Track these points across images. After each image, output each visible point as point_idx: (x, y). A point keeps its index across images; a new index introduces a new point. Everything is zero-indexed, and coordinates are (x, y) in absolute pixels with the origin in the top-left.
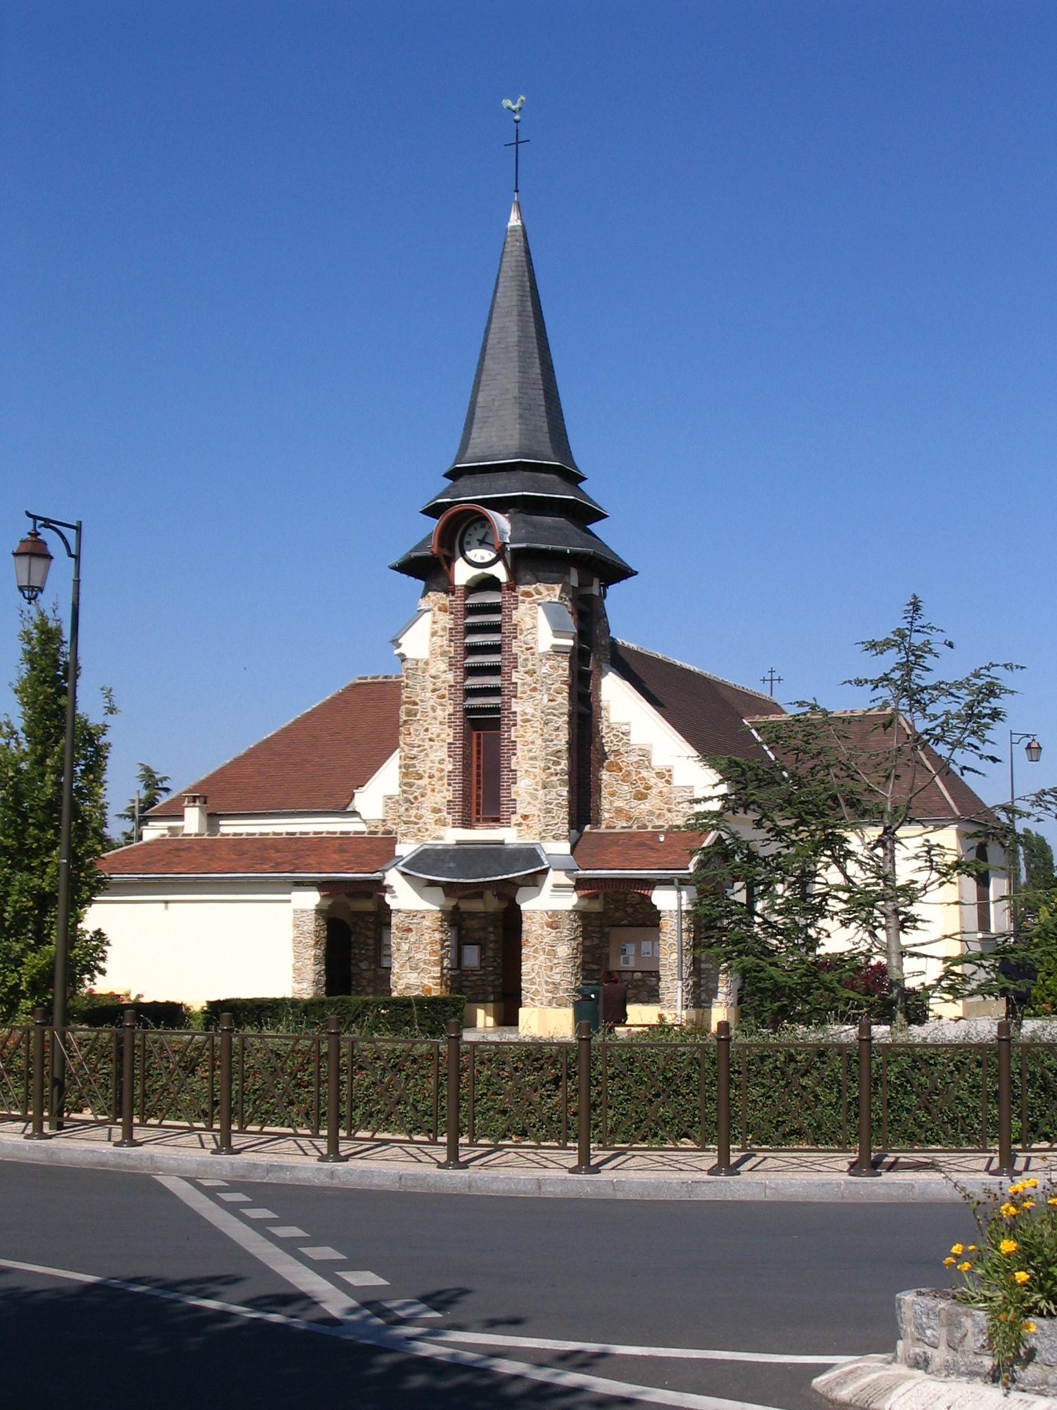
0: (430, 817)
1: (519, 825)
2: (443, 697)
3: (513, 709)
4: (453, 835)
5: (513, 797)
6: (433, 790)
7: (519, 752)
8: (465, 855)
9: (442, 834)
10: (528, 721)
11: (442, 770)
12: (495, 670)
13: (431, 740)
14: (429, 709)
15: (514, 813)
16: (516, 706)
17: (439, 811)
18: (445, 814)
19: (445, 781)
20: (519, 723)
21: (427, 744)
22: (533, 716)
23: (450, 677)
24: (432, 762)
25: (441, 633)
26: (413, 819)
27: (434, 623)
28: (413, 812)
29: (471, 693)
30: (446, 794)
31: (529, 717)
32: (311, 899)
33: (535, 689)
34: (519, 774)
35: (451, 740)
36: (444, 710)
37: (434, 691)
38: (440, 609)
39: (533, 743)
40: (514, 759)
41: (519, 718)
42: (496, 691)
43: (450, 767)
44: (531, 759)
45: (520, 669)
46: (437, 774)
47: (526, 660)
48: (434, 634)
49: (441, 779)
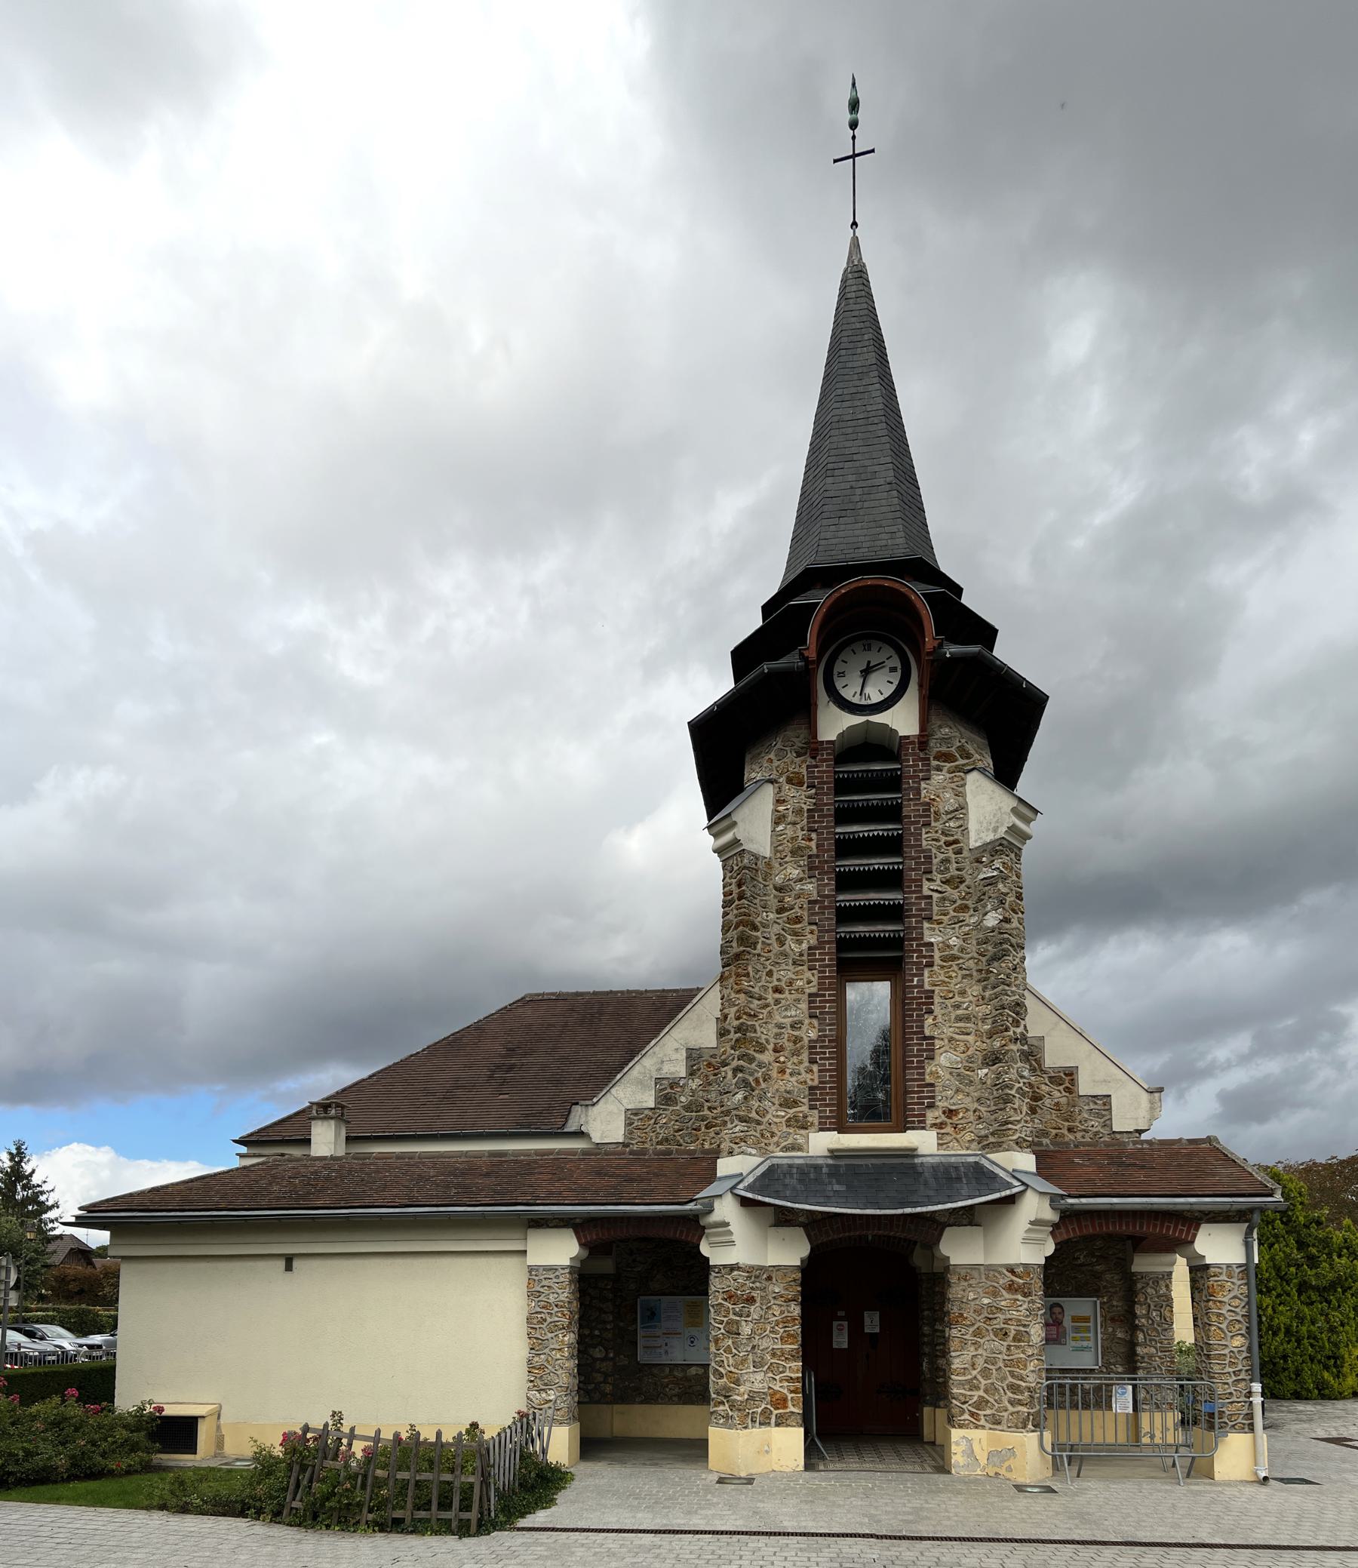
0: (777, 1115)
1: (940, 1126)
2: (798, 920)
3: (927, 939)
4: (821, 1143)
5: (928, 1079)
6: (782, 1071)
7: (936, 1008)
8: (846, 1167)
9: (801, 1141)
10: (954, 958)
11: (797, 1040)
12: (893, 880)
13: (777, 990)
14: (773, 940)
15: (931, 1106)
16: (932, 936)
17: (795, 1103)
18: (805, 1108)
19: (805, 1056)
20: (937, 960)
21: (771, 997)
22: (962, 950)
23: (810, 887)
24: (780, 1026)
25: (791, 818)
26: (753, 1115)
27: (779, 802)
28: (755, 1103)
29: (845, 915)
30: (805, 1076)
31: (955, 952)
32: (560, 1251)
33: (964, 908)
34: (938, 1043)
35: (814, 990)
36: (800, 942)
37: (780, 911)
38: (789, 781)
39: (963, 993)
40: (929, 1021)
41: (937, 955)
42: (895, 913)
43: (813, 1034)
44: (959, 1019)
45: (938, 877)
46: (789, 1046)
47: (947, 860)
48: (779, 819)
49: (796, 1053)
